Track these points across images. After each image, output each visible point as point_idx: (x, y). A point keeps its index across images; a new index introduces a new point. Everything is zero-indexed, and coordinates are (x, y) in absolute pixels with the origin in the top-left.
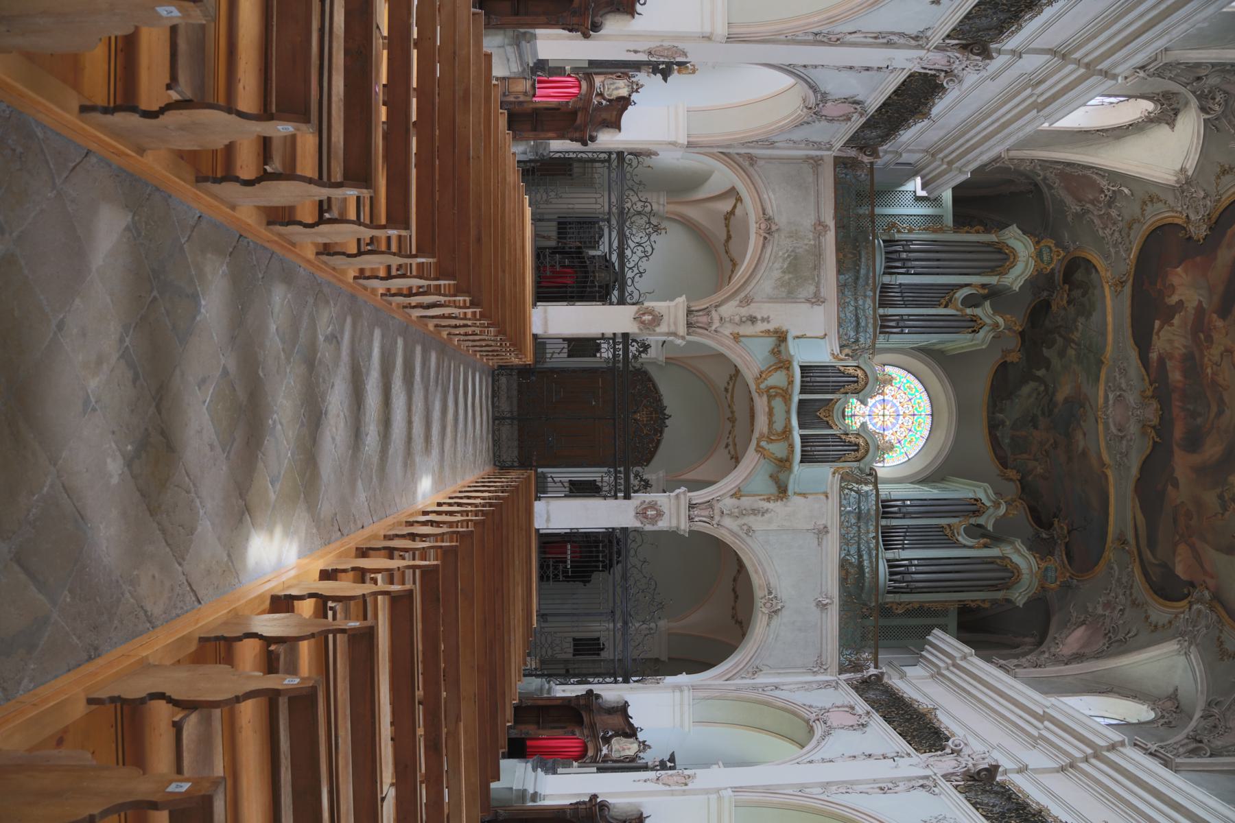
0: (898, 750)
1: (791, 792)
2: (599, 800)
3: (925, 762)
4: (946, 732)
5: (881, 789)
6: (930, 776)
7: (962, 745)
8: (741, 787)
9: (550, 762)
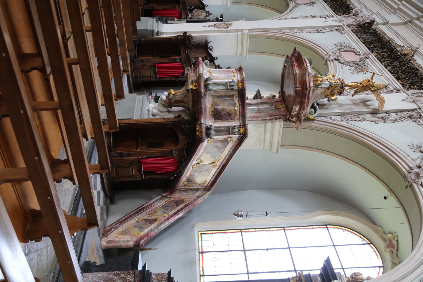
0: (328, 14)
1: (275, 31)
2: (187, 35)
3: (339, 19)
4: (353, 7)
5: (317, 31)
6: (341, 25)
8: (253, 29)
9: (165, 18)
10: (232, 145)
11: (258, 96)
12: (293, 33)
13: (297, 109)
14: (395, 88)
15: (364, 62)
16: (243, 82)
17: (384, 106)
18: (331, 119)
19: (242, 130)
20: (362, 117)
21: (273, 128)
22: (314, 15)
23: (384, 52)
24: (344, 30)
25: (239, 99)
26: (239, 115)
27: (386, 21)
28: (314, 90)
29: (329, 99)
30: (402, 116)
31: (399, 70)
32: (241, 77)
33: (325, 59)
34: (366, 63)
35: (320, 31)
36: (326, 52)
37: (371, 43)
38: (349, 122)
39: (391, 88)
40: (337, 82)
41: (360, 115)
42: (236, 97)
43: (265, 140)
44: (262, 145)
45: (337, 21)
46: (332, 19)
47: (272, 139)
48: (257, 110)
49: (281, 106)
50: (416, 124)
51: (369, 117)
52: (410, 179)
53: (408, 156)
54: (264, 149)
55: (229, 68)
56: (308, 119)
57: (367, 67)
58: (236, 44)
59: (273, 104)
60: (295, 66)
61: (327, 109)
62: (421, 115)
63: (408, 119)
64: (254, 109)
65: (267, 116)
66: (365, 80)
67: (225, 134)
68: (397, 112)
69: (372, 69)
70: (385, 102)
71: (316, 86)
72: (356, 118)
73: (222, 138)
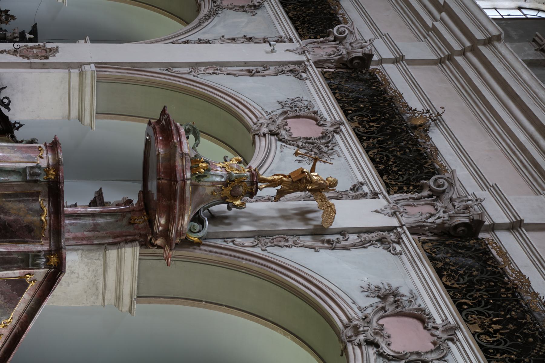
3: (302, 48)
7: (347, 32)
10: (34, 290)
11: (98, 202)
12: (196, 74)
13: (163, 221)
14: (372, 189)
15: (328, 139)
16: (57, 165)
17: (334, 219)
18: (234, 244)
19: (54, 260)
20: (293, 240)
21: (120, 260)
22: (251, 36)
23: (373, 121)
24: (307, 72)
25: (49, 201)
26: (50, 230)
27: (398, 56)
28: (195, 187)
29: (230, 204)
30: (367, 239)
31: (391, 157)
32: (54, 159)
33: (252, 133)
34: (334, 141)
35: (253, 72)
36: (256, 117)
37: (356, 100)
38: (267, 248)
39: (366, 189)
40: (243, 172)
41: (292, 237)
42: (44, 196)
43: (105, 286)
44: (100, 297)
45: (298, 51)
46: (288, 46)
47: (119, 283)
48: (93, 226)
49: (141, 220)
50: (388, 252)
51: (307, 240)
52: (344, 338)
53: (354, 303)
54: (103, 304)
55: (32, 142)
56: (187, 243)
57: (332, 149)
58: (67, 95)
59: (124, 216)
60: (159, 141)
61: (229, 224)
62: (401, 238)
63: (376, 245)
64: (85, 225)
65: (109, 236)
66: (298, 170)
67: (18, 268)
68: (360, 231)
69: (341, 155)
70: (335, 213)
71: (197, 177)
72: (280, 241)
73: (13, 276)
